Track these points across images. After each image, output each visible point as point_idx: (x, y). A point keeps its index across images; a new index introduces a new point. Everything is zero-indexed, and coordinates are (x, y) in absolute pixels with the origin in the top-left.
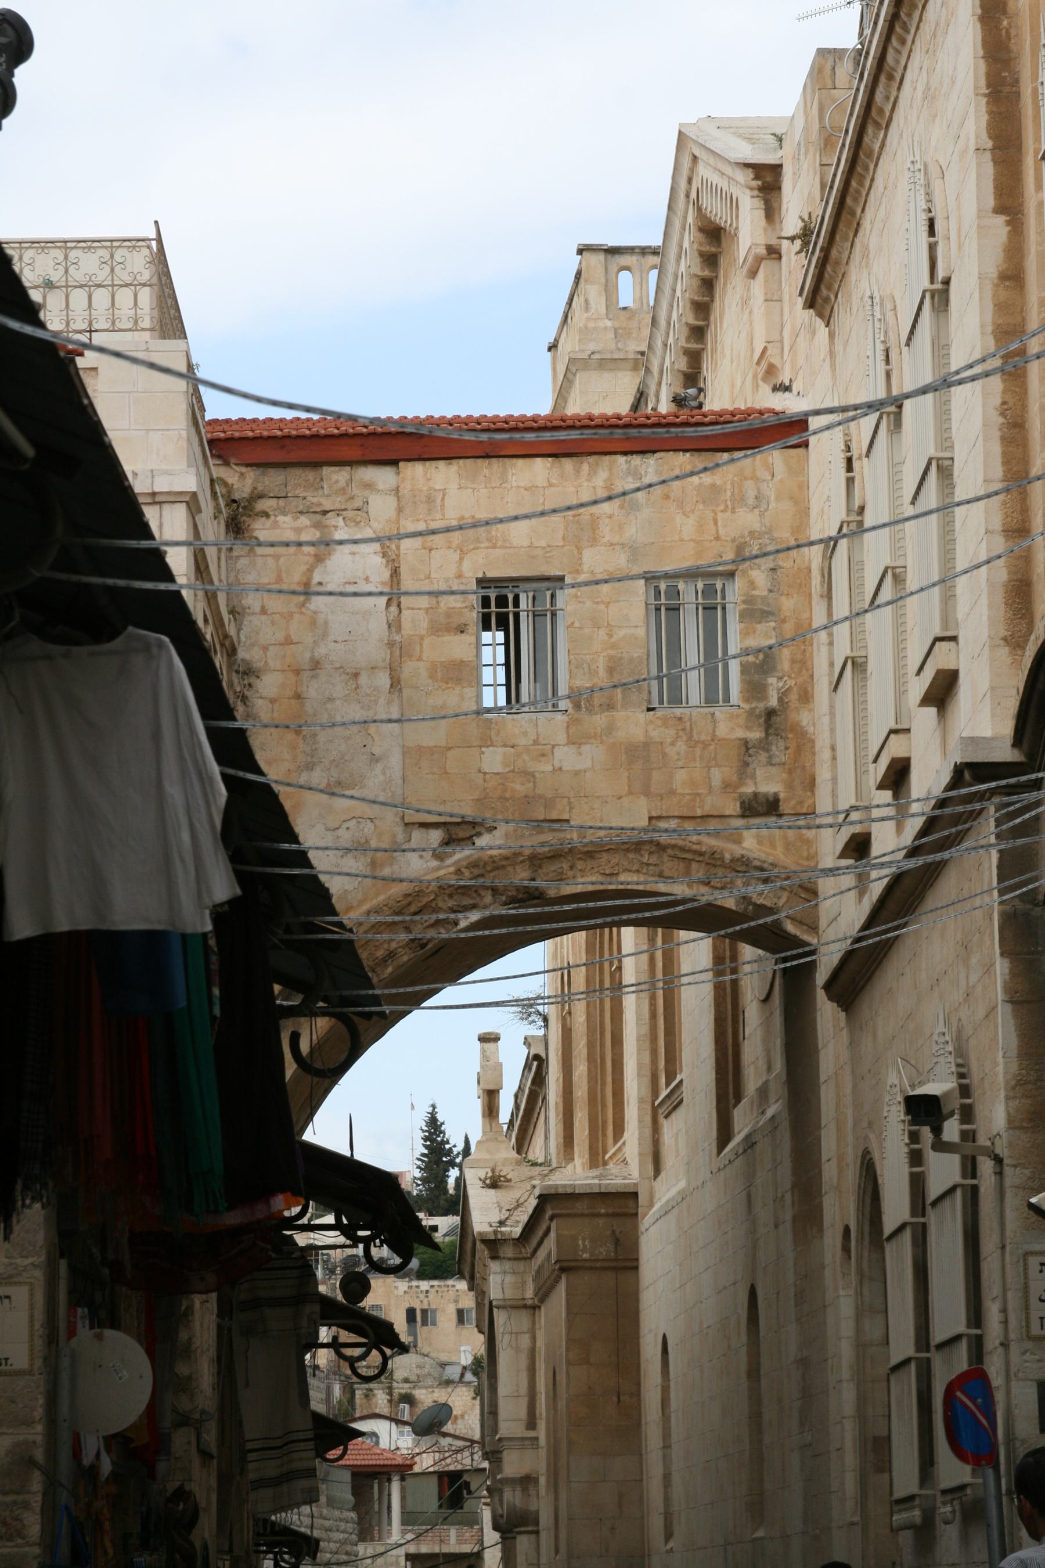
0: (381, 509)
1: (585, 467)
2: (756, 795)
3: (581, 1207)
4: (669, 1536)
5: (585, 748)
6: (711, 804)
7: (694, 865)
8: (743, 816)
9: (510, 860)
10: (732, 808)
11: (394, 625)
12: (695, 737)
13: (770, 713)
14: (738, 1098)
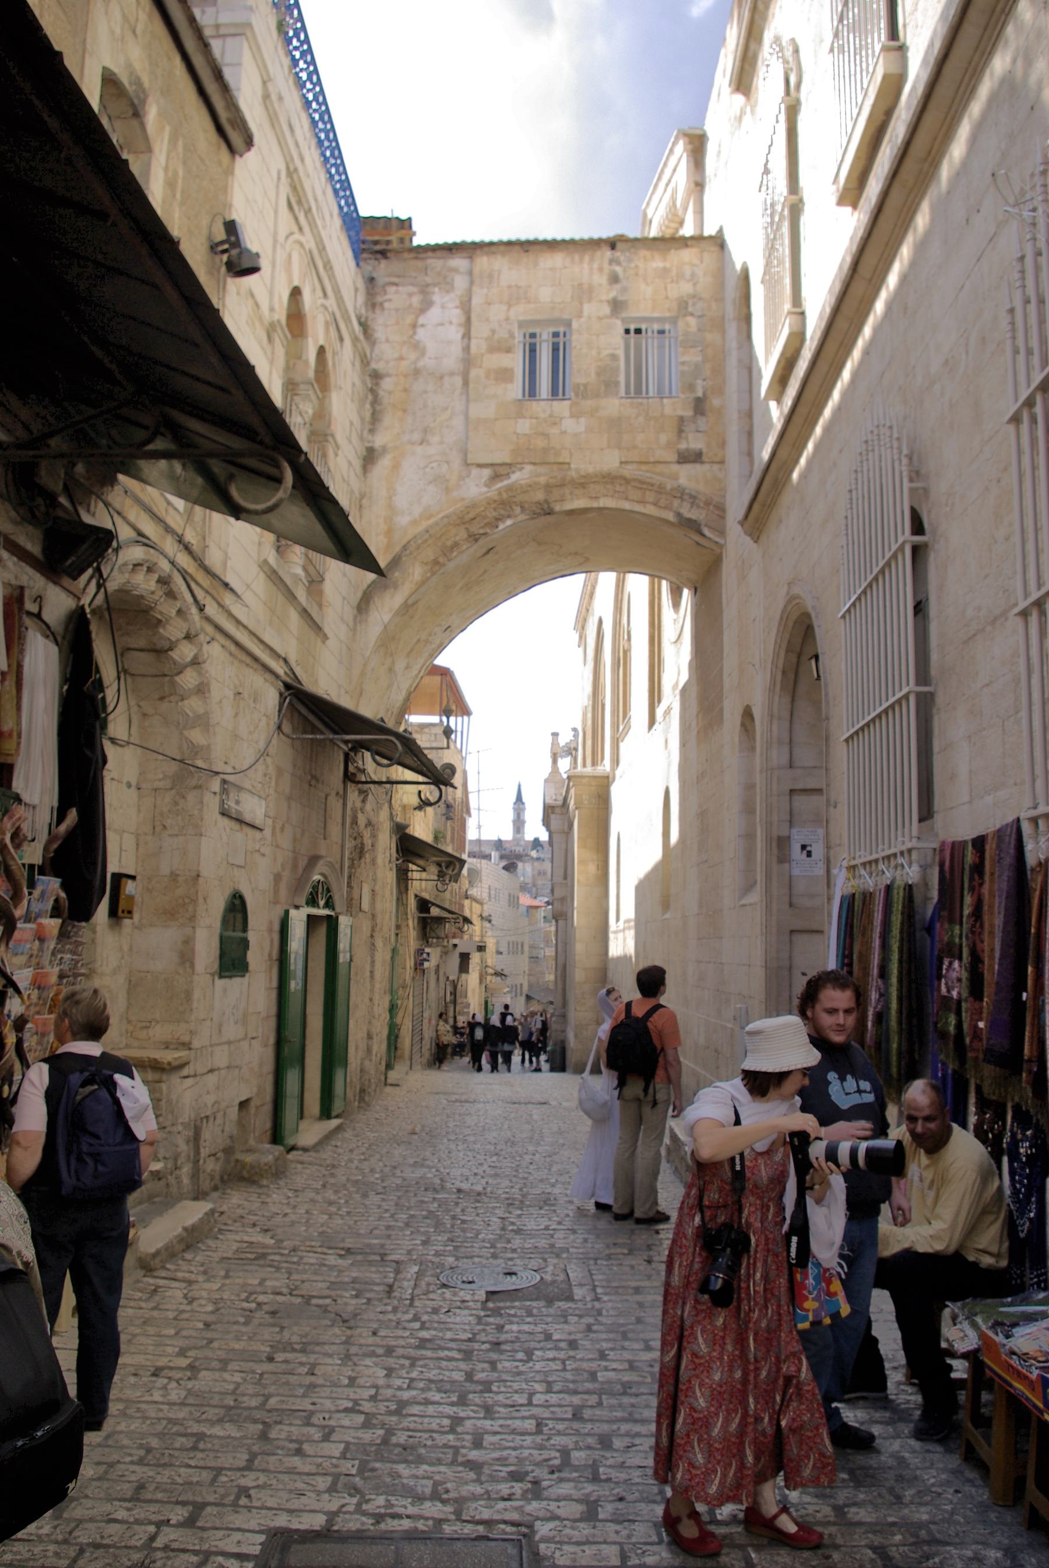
0: (460, 282)
1: (587, 258)
2: (687, 450)
3: (585, 781)
4: (618, 920)
5: (583, 420)
8: (679, 462)
9: (531, 487)
10: (674, 457)
11: (467, 349)
14: (659, 701)
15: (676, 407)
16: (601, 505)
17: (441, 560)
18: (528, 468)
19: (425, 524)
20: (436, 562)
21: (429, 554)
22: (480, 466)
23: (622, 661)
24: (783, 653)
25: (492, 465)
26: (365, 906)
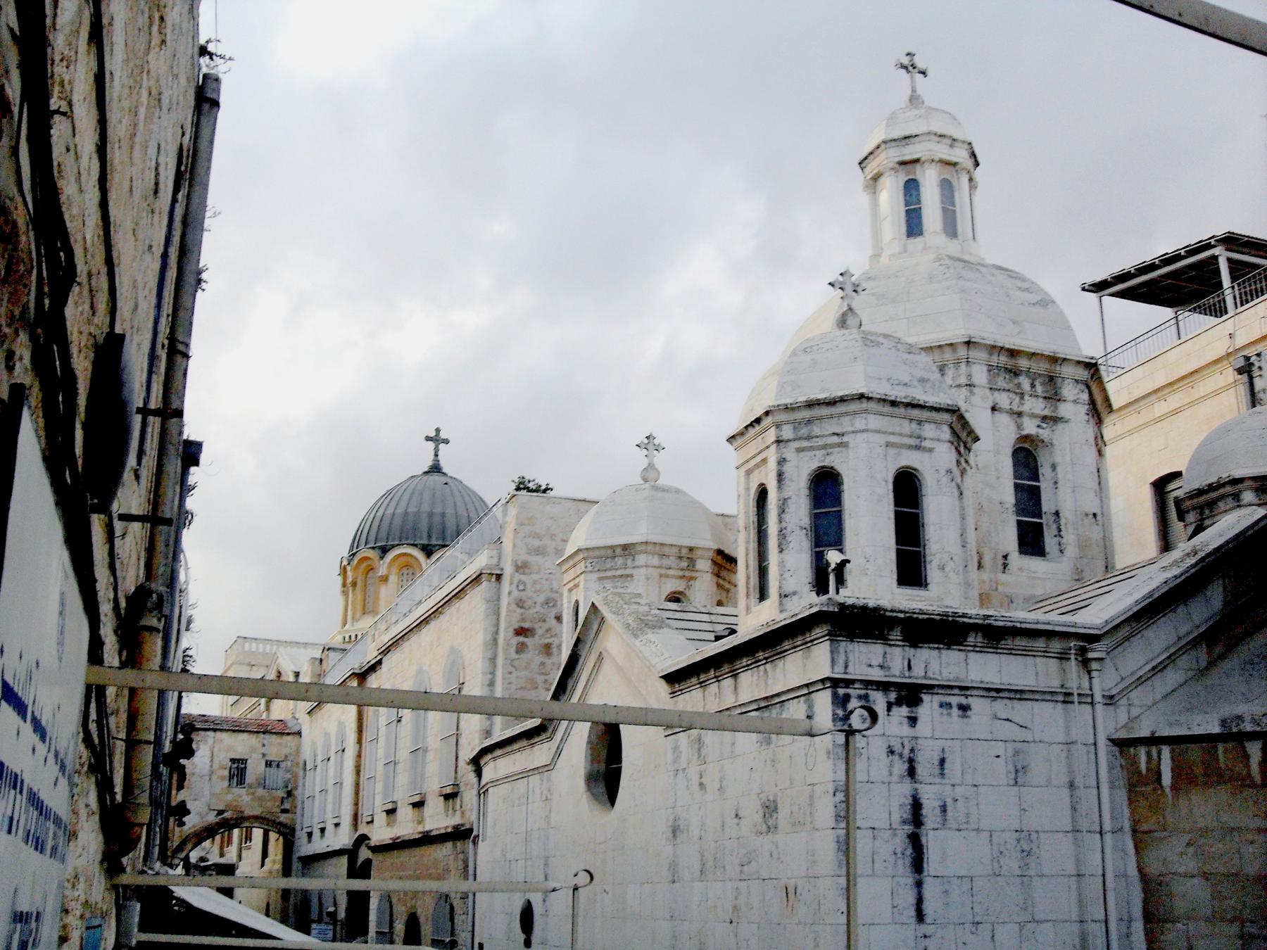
0: (210, 741)
15: (281, 794)
21: (194, 840)
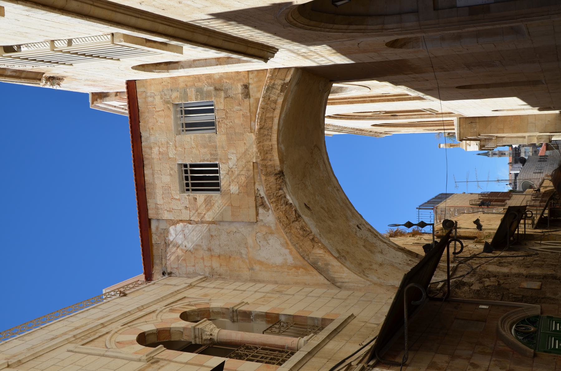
0: (162, 226)
2: (242, 93)
6: (246, 111)
7: (267, 116)
8: (250, 98)
12: (224, 116)
13: (216, 89)
14: (408, 95)
16: (276, 143)
17: (311, 237)
18: (257, 186)
19: (291, 247)
20: (313, 240)
22: (257, 214)
23: (394, 114)
24: (336, 26)
25: (256, 207)
26: (536, 285)
